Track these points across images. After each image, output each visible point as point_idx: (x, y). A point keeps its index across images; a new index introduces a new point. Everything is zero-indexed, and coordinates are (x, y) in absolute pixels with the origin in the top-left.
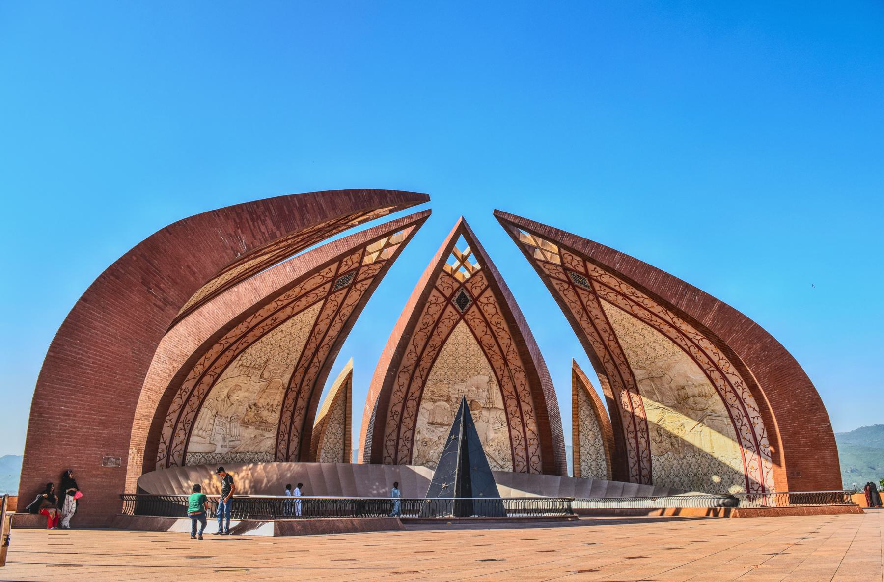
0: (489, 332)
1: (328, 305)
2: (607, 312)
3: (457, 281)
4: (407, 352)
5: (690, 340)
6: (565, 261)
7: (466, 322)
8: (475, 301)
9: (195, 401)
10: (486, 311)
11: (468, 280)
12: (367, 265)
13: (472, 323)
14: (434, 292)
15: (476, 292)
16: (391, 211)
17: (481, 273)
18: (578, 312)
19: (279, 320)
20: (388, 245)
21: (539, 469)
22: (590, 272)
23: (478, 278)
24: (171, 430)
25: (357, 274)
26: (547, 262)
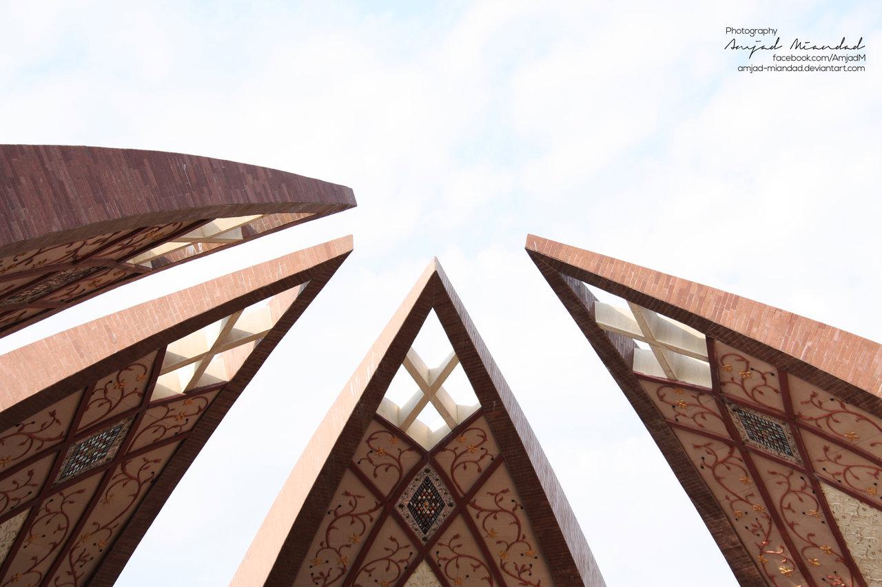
1: (38, 528)
2: (842, 524)
3: (414, 446)
6: (726, 377)
7: (435, 568)
8: (463, 503)
10: (492, 534)
11: (442, 446)
12: (165, 402)
13: (452, 571)
14: (349, 482)
15: (465, 480)
16: (249, 234)
17: (482, 423)
18: (756, 529)
20: (224, 343)
23: (471, 437)
26: (672, 384)
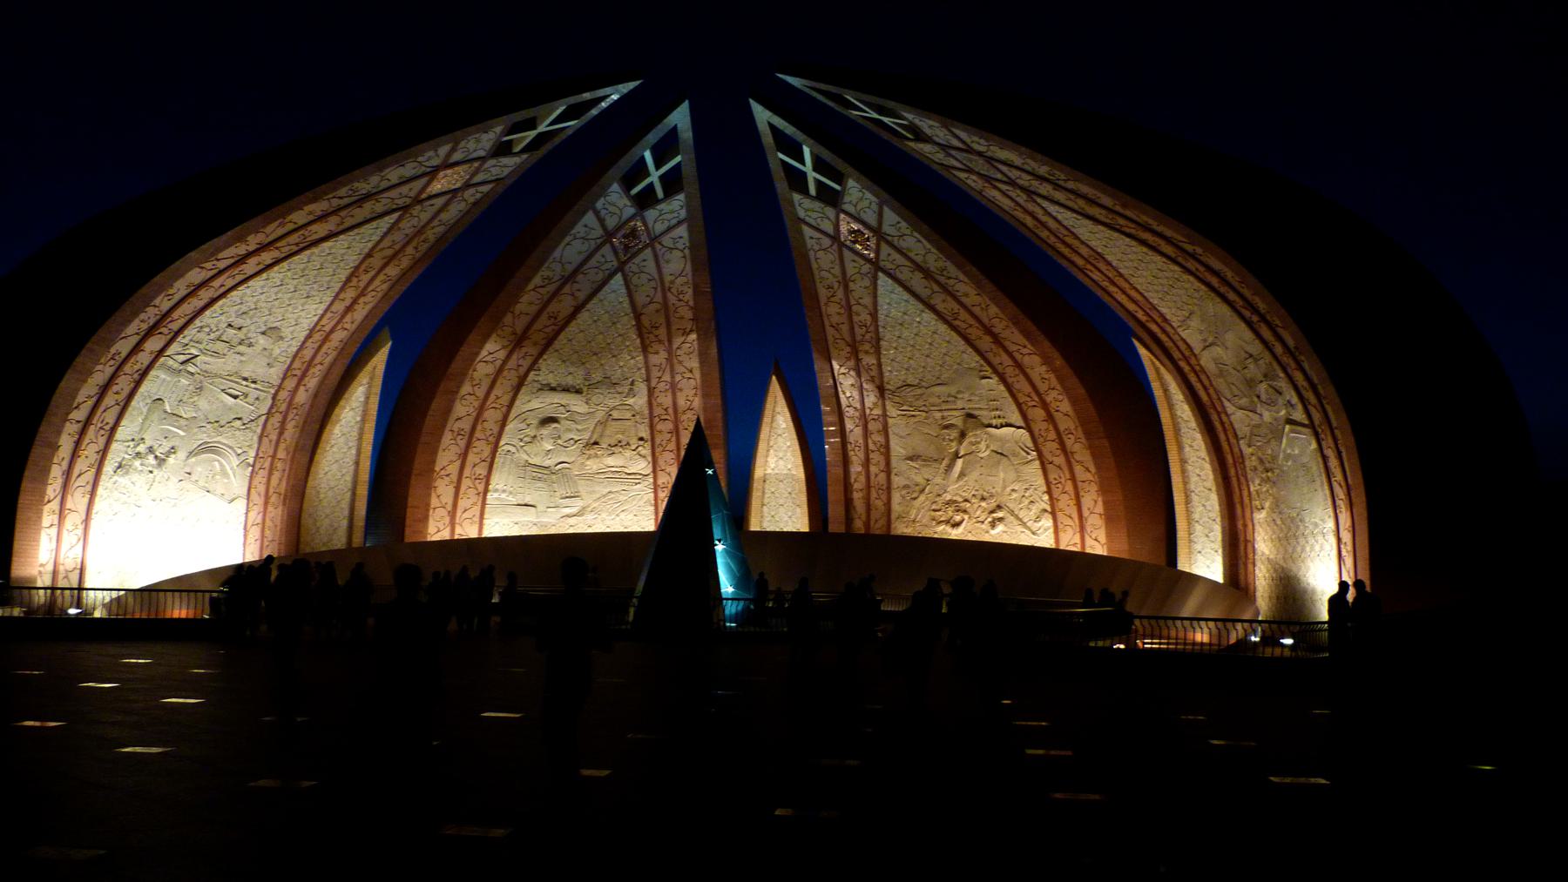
0: (936, 288)
1: (635, 280)
4: (830, 339)
5: (1193, 256)
8: (877, 231)
9: (481, 448)
13: (899, 275)
14: (807, 231)
15: (871, 218)
19: (561, 316)
21: (1103, 538)
22: (975, 146)
24: (451, 490)
25: (645, 224)
